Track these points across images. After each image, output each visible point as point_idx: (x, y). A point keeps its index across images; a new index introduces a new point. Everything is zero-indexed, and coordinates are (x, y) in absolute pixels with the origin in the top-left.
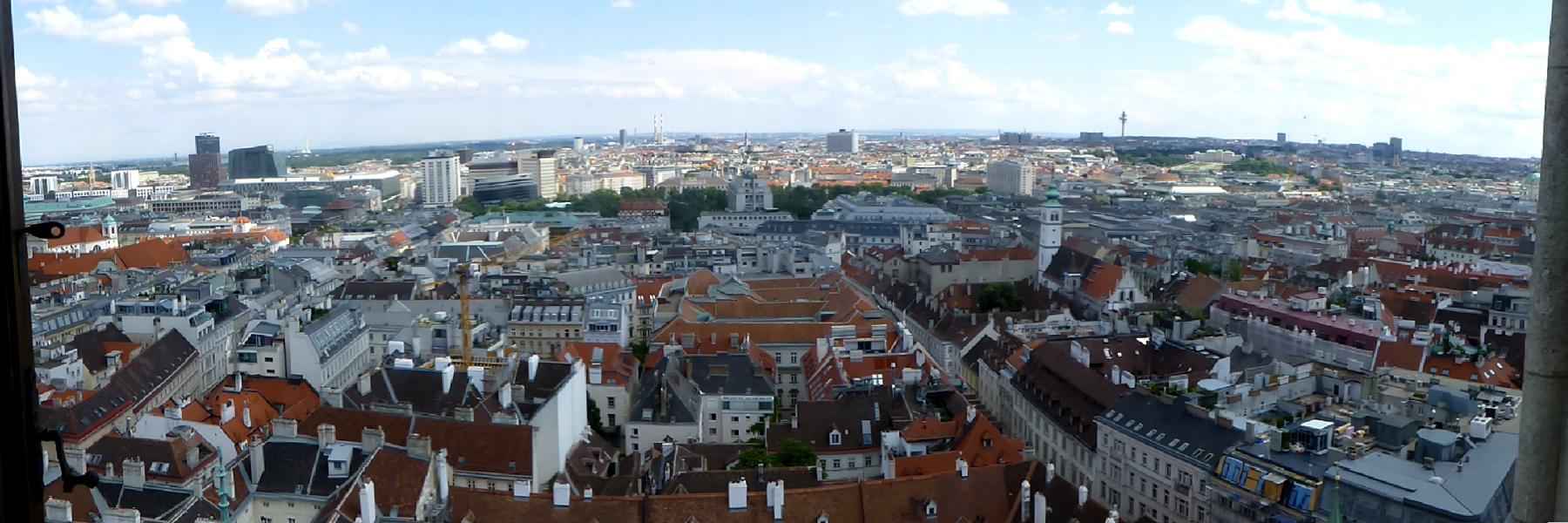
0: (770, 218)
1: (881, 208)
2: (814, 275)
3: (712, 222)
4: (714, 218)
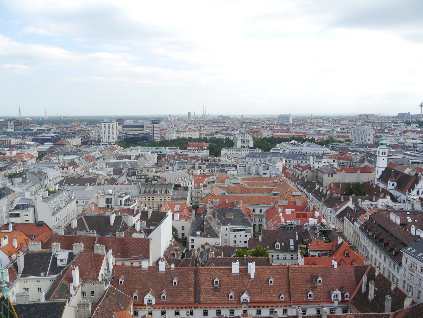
0: (252, 151)
1: (302, 148)
2: (271, 176)
3: (227, 153)
4: (228, 151)
